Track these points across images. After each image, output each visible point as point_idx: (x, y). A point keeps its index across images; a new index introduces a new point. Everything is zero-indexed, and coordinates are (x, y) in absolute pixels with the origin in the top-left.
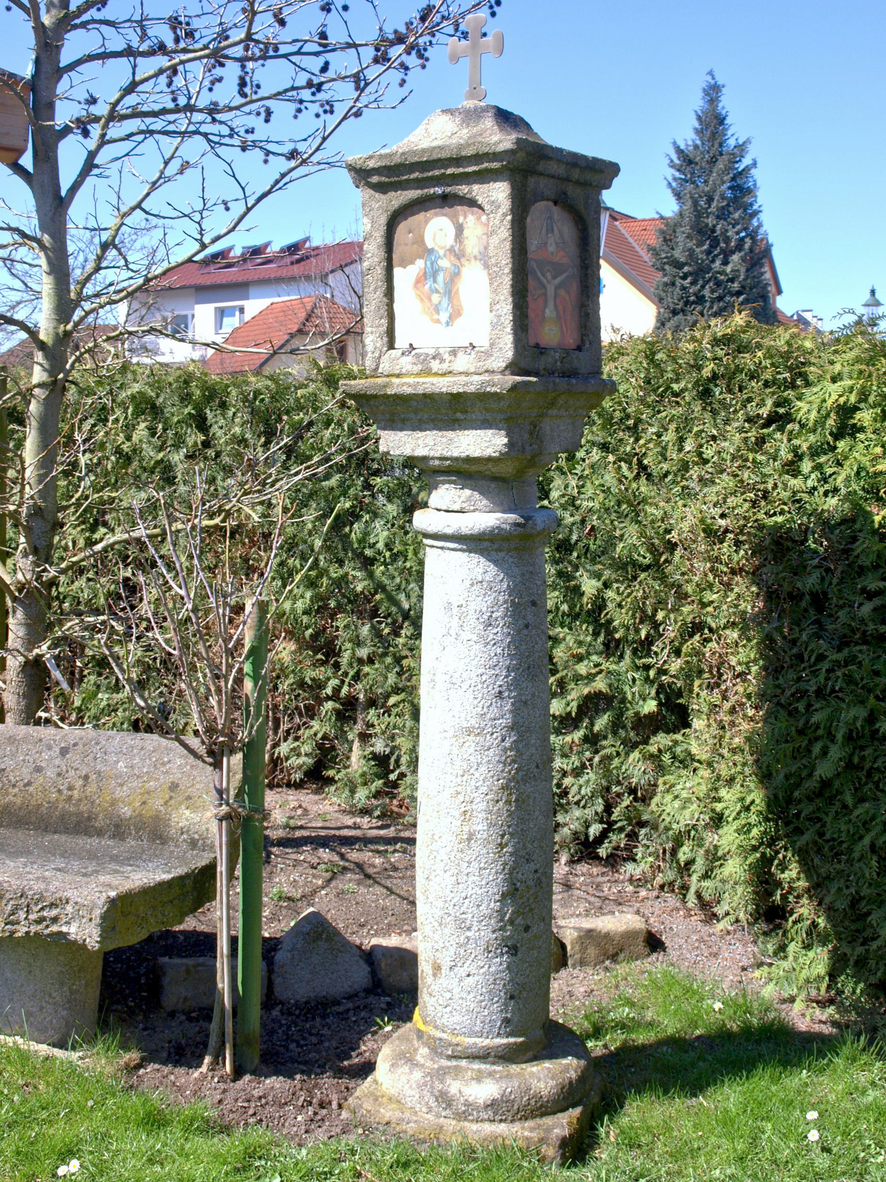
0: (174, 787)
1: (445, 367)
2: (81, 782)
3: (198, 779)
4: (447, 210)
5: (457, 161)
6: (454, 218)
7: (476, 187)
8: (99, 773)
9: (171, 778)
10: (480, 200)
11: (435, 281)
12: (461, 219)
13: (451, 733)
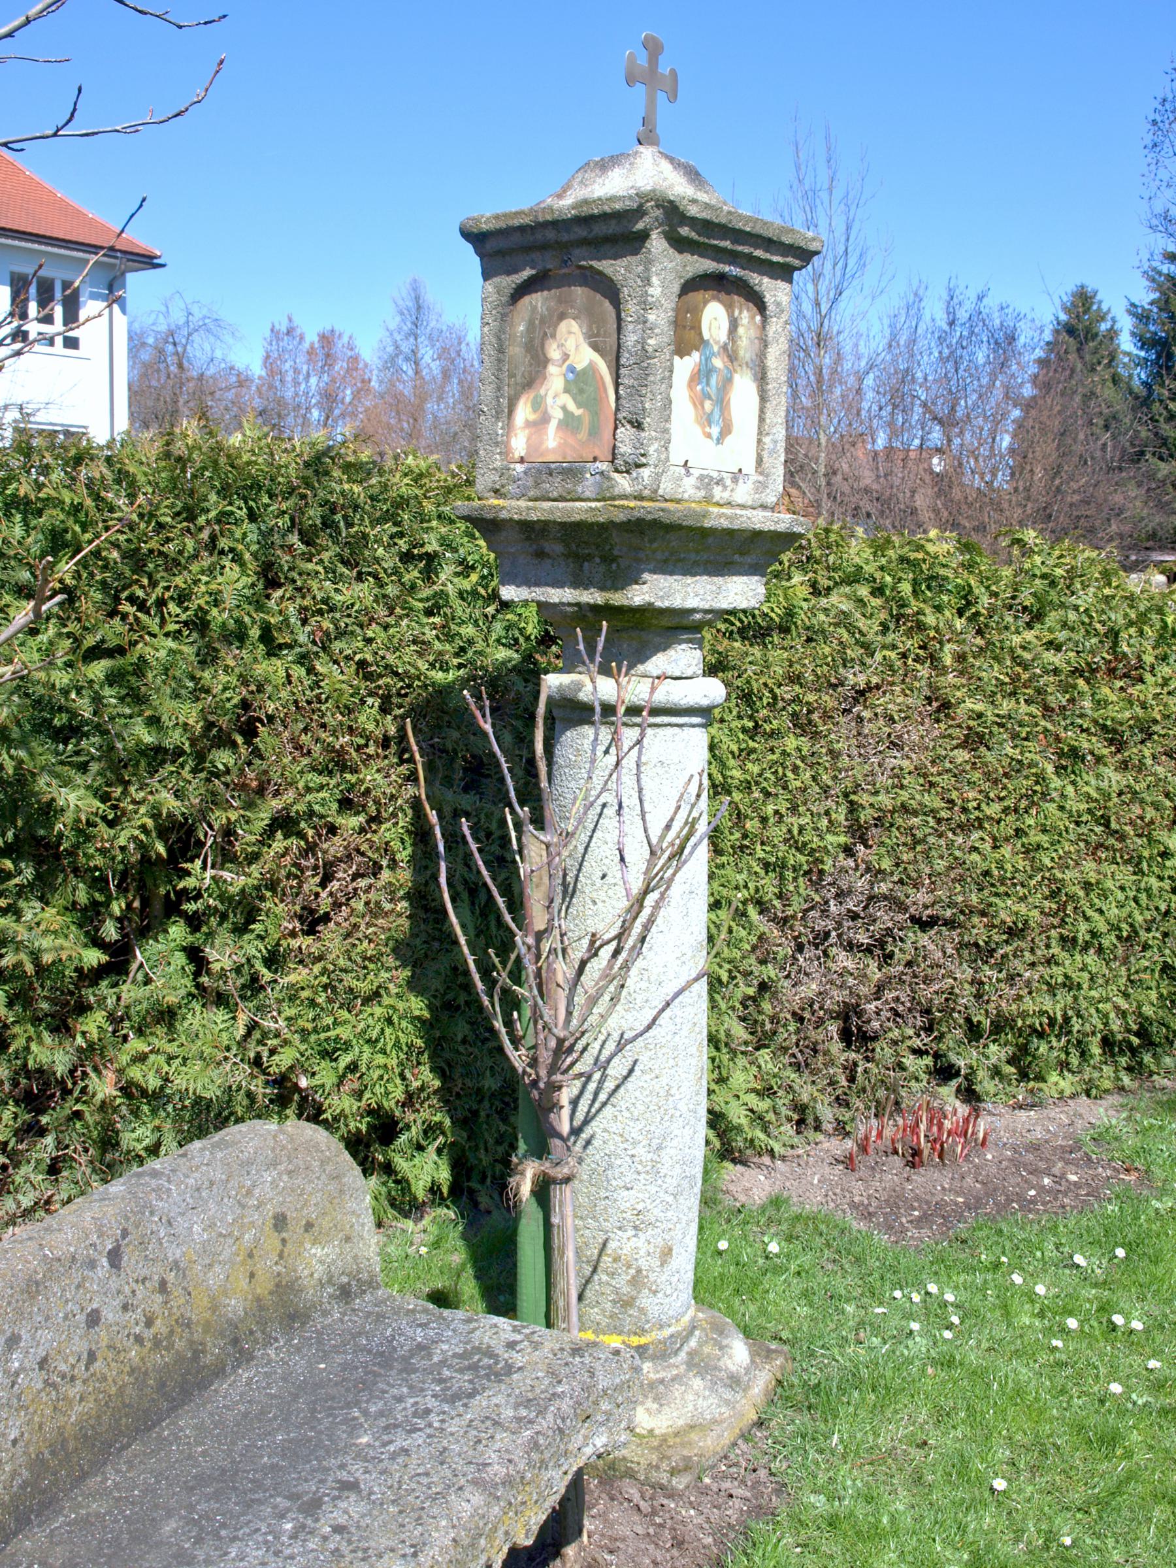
0: (280, 1222)
1: (726, 495)
2: (159, 1299)
3: (309, 1188)
4: (722, 295)
5: (769, 243)
6: (729, 308)
7: (766, 280)
8: (176, 1265)
9: (270, 1210)
10: (769, 299)
11: (708, 384)
12: (736, 313)
13: (690, 954)
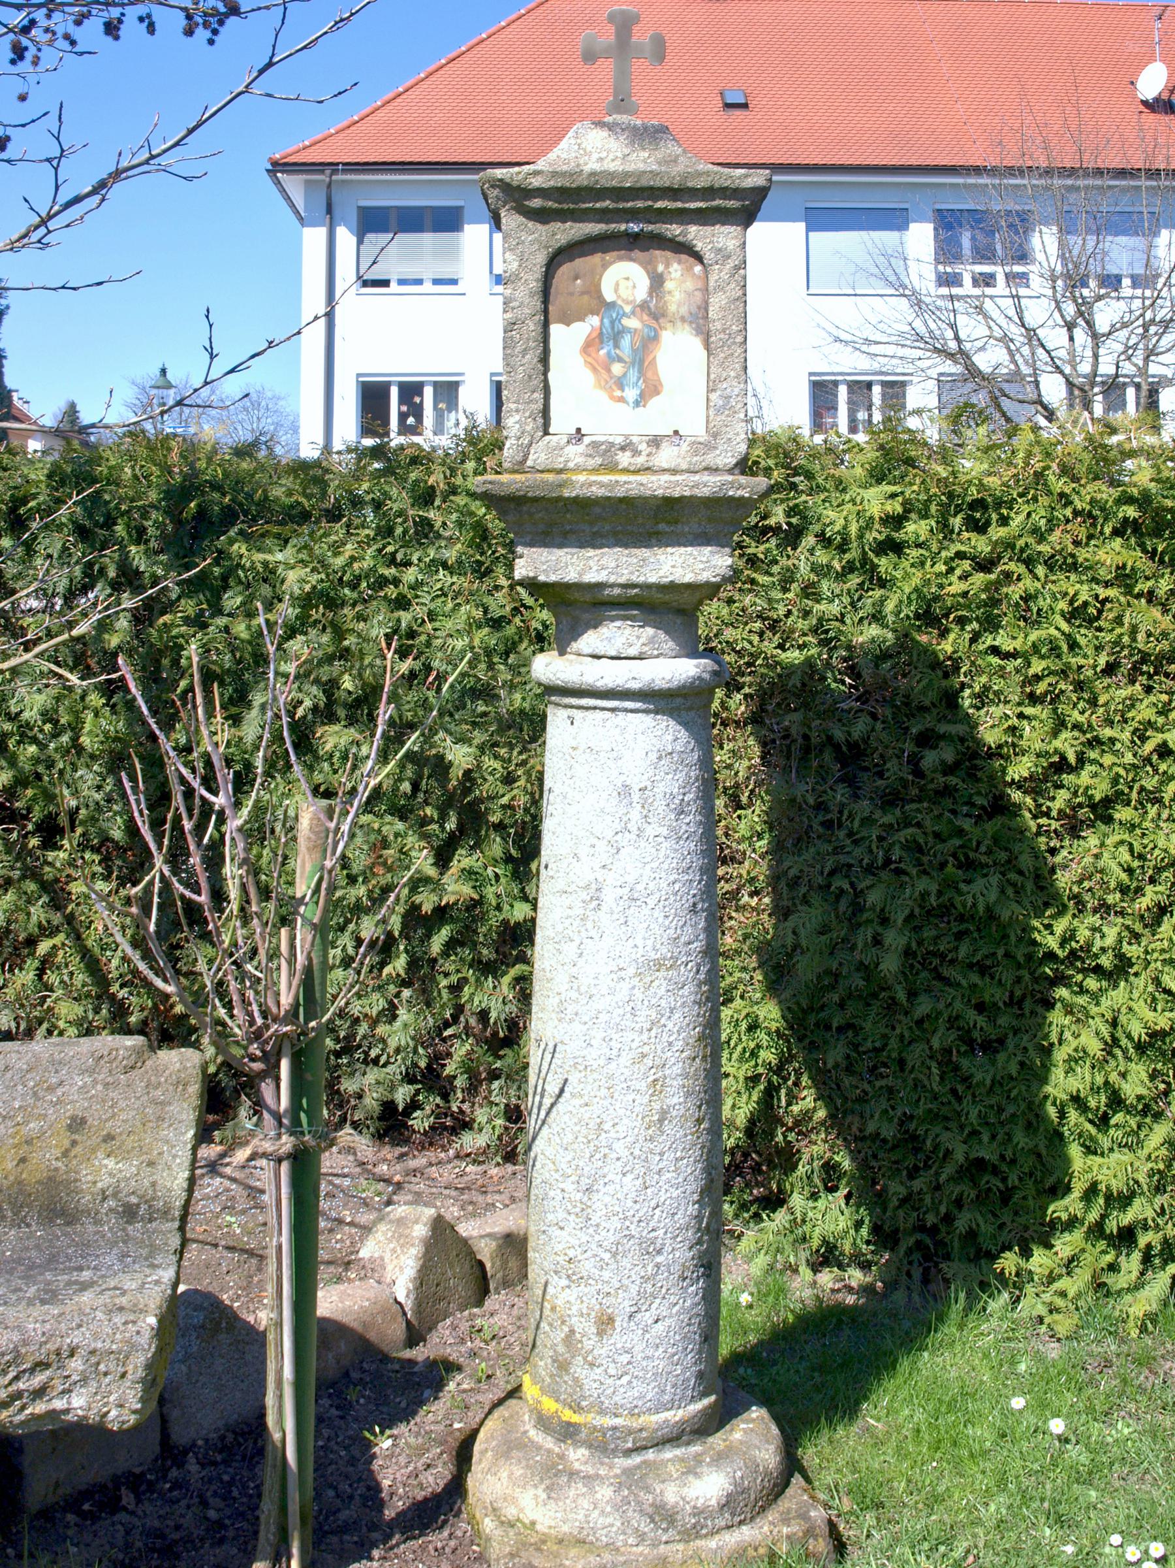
1: (640, 460)
3: (122, 1104)
4: (637, 253)
7: (693, 229)
10: (699, 246)
11: (617, 346)
12: (661, 268)
13: (632, 971)
